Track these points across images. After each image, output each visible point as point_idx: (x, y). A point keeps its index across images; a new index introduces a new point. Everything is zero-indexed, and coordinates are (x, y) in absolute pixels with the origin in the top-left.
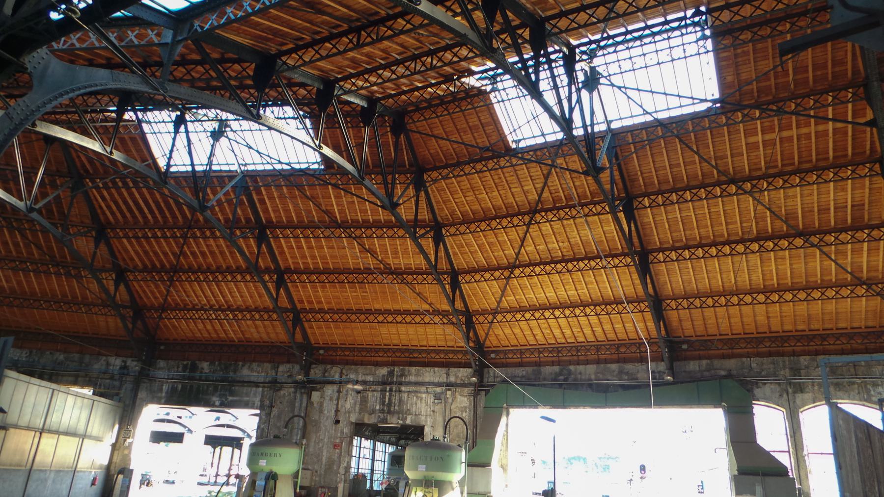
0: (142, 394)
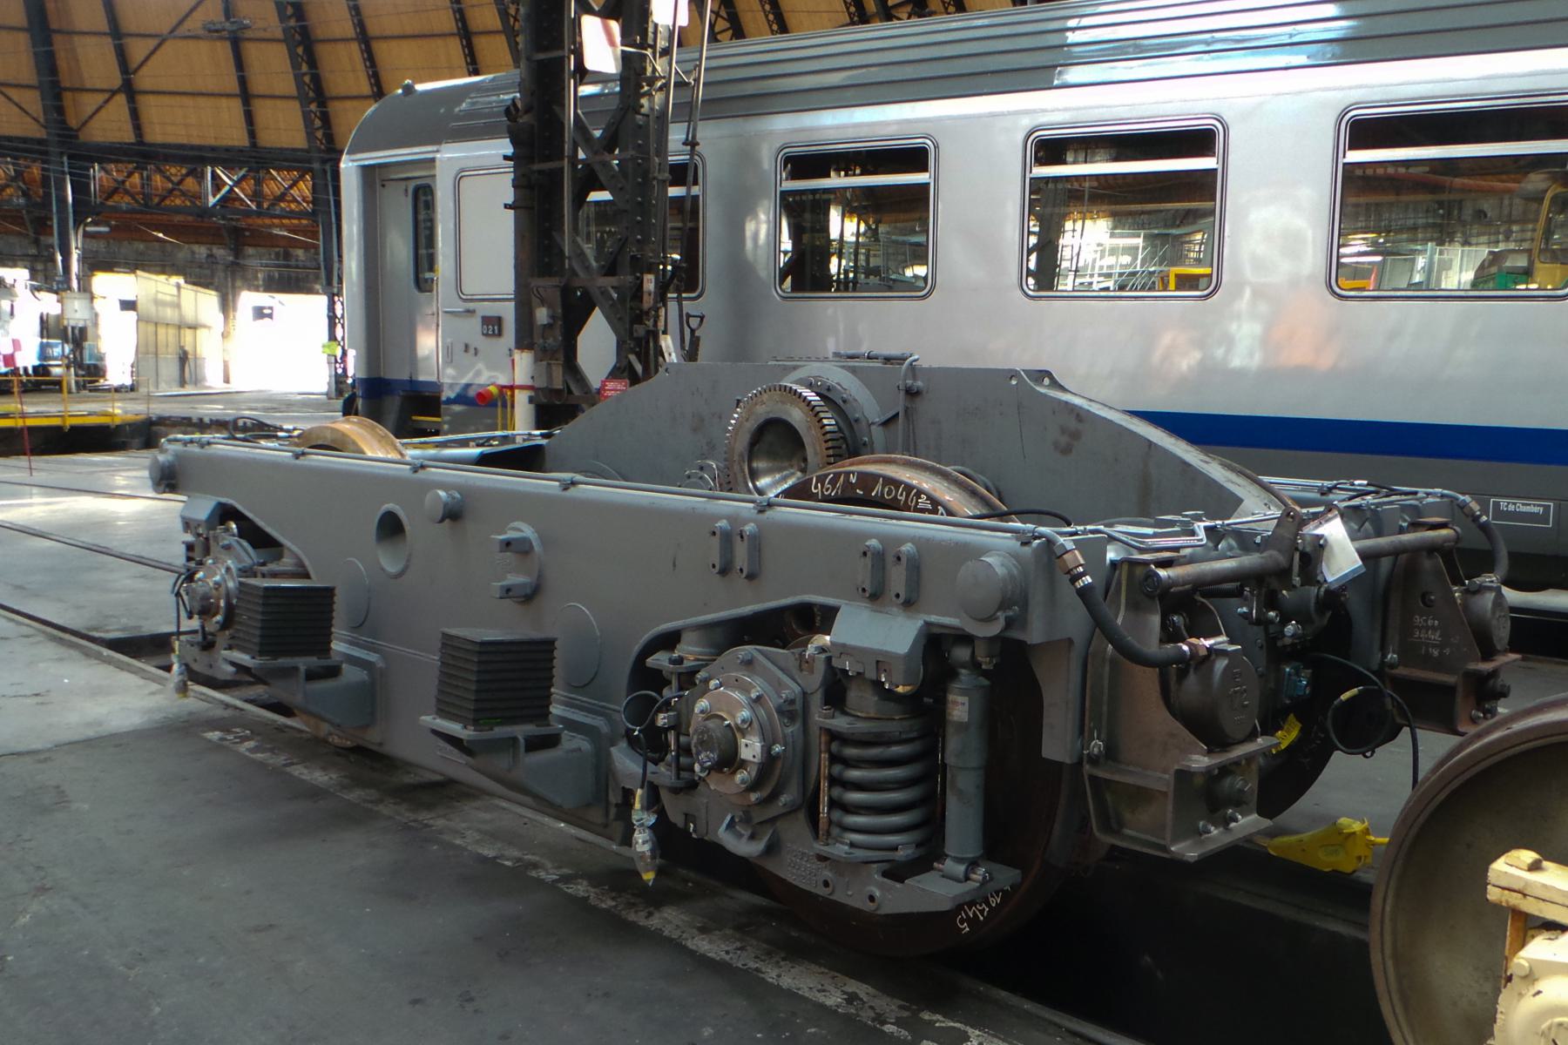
0: (239, 283)
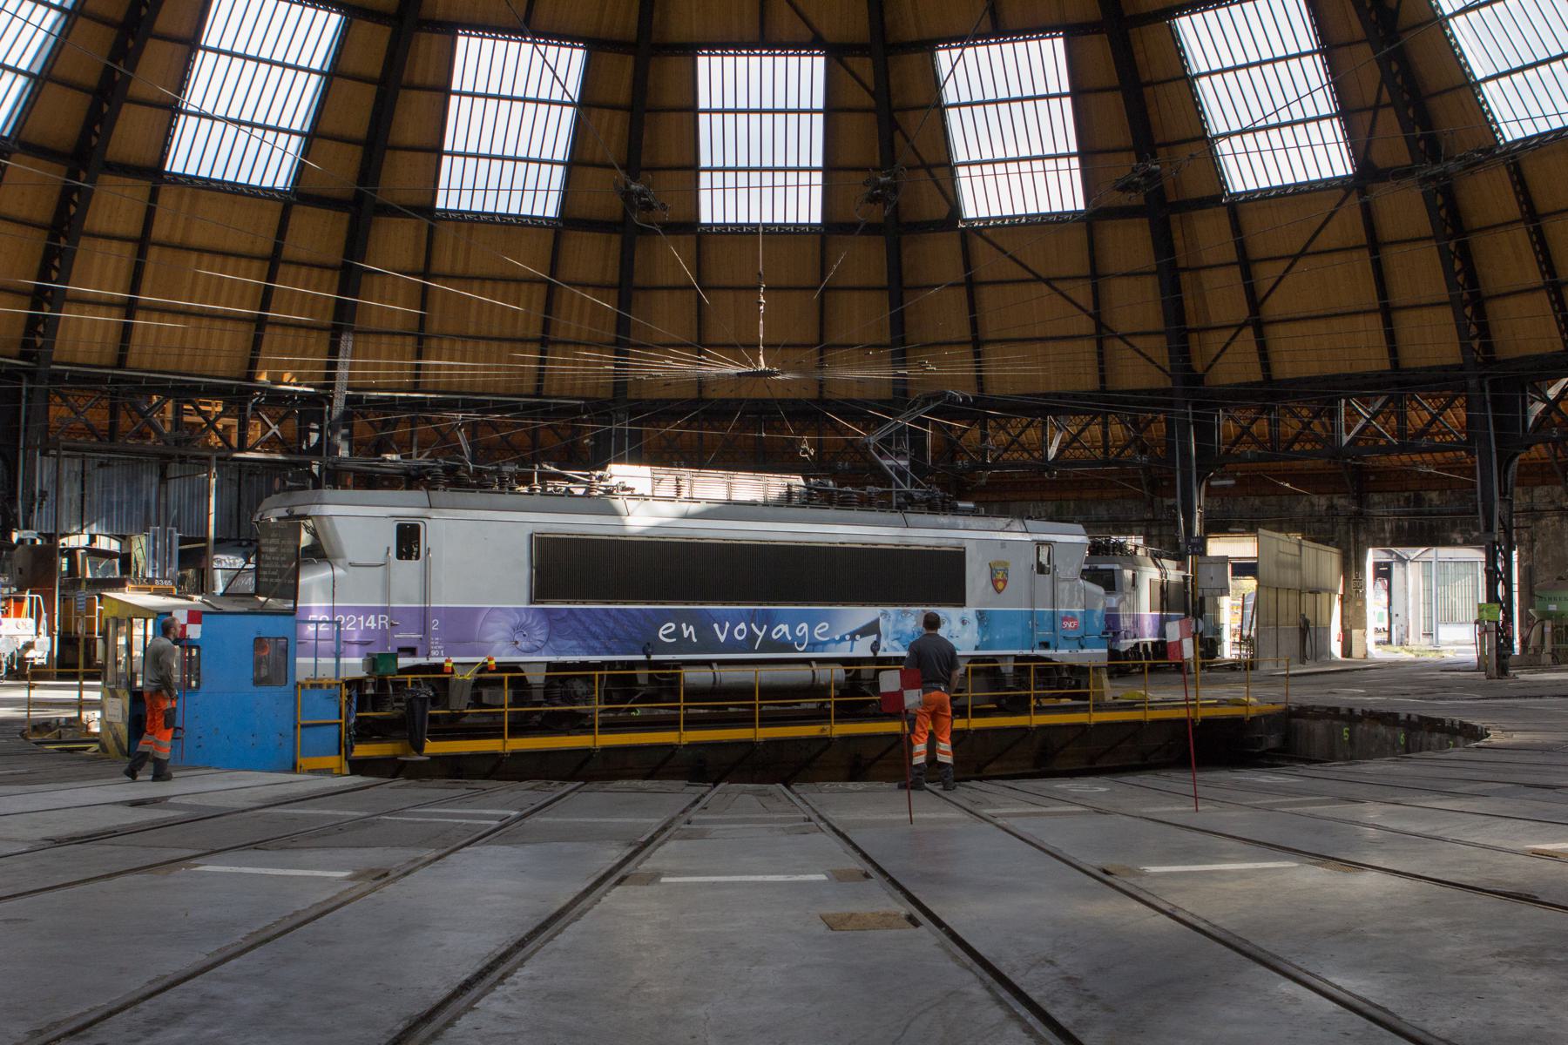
0: (1362, 537)
